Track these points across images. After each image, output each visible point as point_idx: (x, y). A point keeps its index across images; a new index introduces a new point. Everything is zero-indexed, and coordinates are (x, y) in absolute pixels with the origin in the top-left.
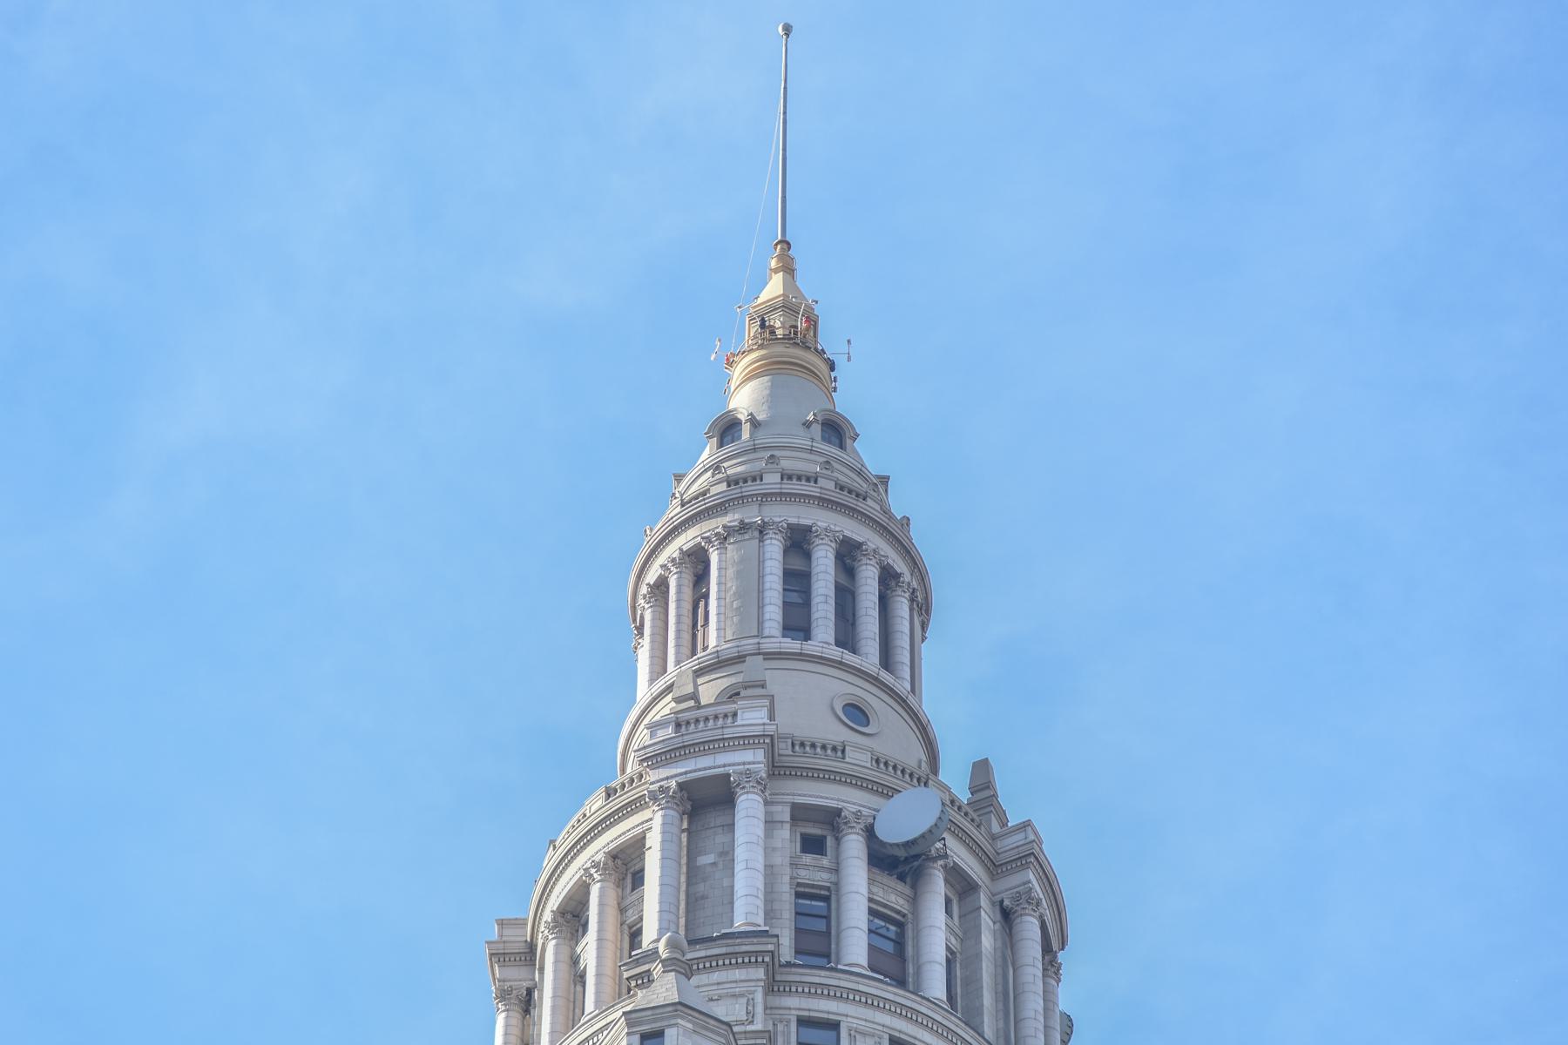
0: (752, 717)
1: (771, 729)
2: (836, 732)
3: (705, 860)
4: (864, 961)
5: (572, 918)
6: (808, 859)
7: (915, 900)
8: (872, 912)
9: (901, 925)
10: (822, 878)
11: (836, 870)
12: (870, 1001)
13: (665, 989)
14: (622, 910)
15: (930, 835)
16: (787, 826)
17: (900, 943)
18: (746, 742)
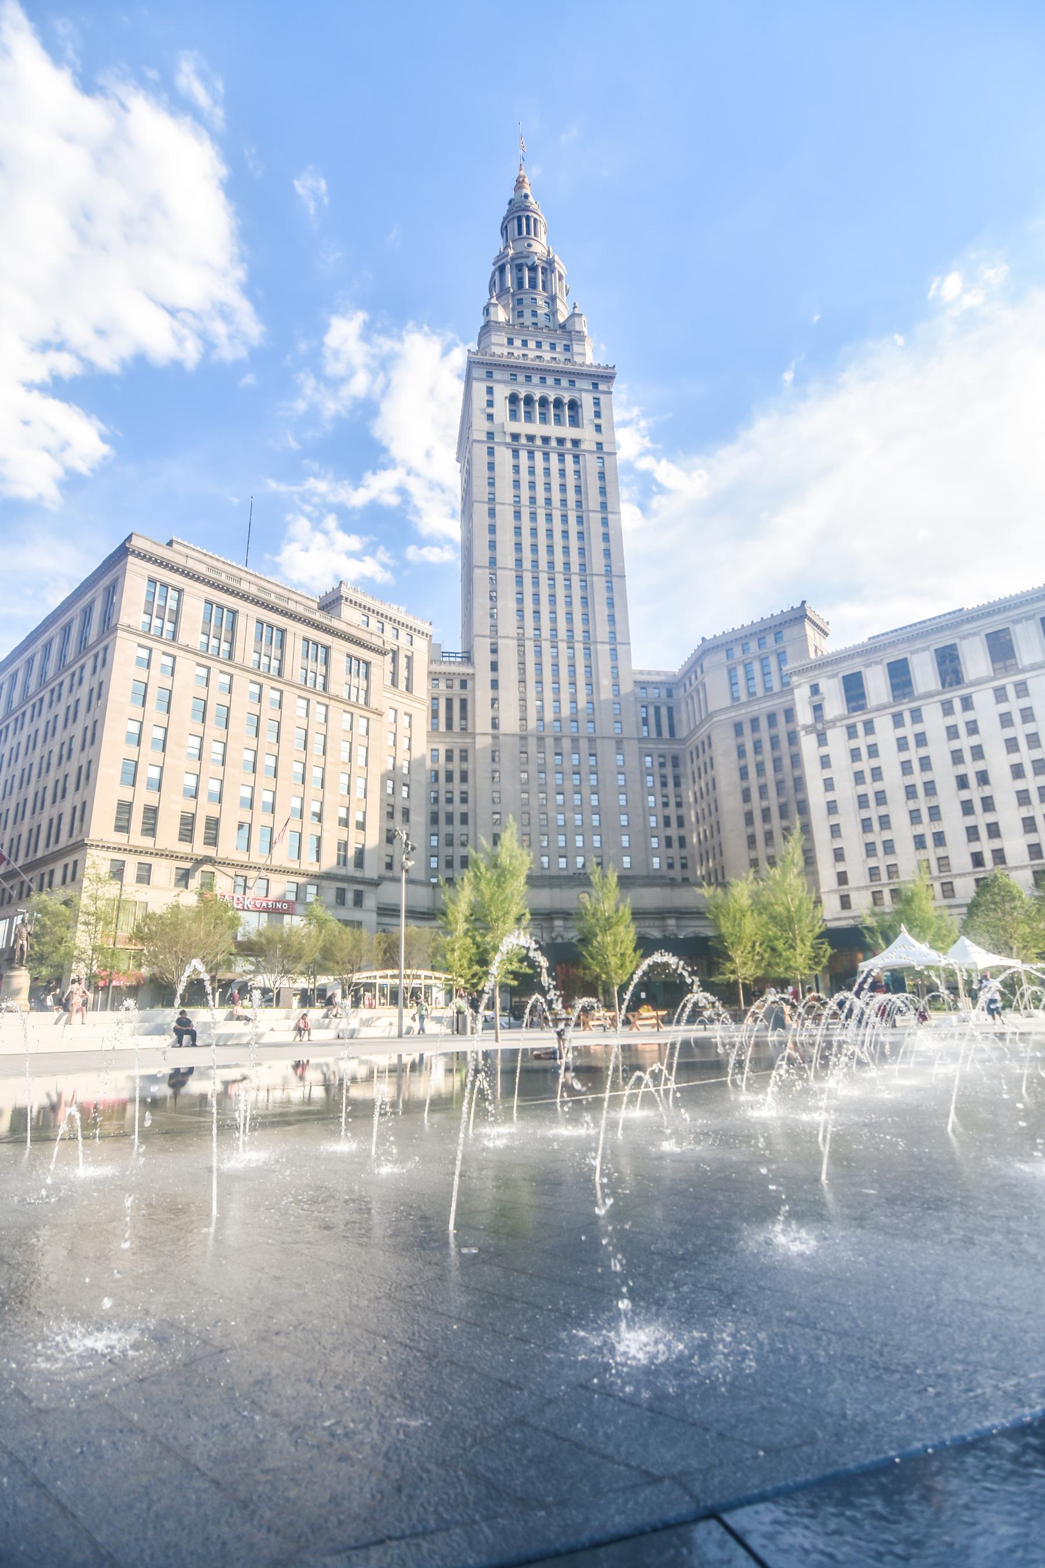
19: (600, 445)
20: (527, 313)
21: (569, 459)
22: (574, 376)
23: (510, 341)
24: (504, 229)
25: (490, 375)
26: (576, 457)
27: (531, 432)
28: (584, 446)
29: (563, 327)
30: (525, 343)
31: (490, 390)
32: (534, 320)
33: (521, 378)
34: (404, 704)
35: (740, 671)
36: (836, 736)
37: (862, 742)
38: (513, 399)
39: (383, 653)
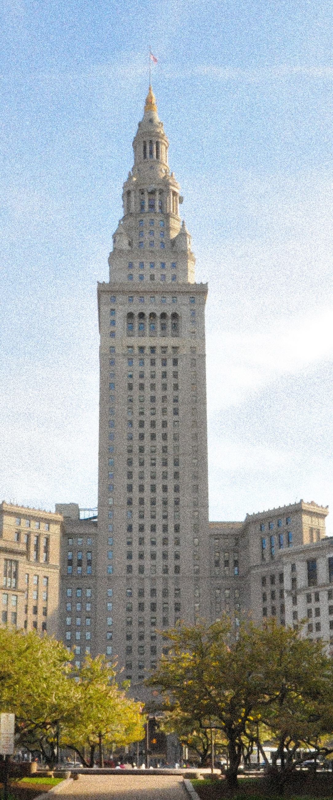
22: (174, 294)
23: (131, 265)
24: (135, 147)
25: (113, 299)
29: (173, 242)
30: (142, 265)
33: (136, 299)
34: (42, 572)
35: (267, 540)
36: (301, 599)
37: (313, 605)
38: (130, 315)
39: (27, 554)
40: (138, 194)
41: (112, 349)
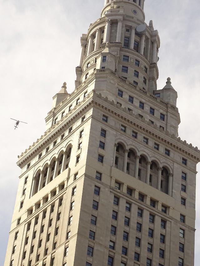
0: (121, 12)
1: (124, 14)
2: (133, 15)
3: (113, 31)
4: (133, 48)
5: (93, 36)
6: (127, 32)
7: (140, 40)
8: (135, 41)
9: (138, 43)
10: (128, 35)
11: (130, 34)
12: (133, 54)
13: (106, 50)
14: (100, 36)
15: (144, 31)
16: (125, 28)
17: (138, 45)
18: (120, 15)
19: (183, 218)
20: (131, 71)
21: (158, 220)
23: (121, 93)
25: (106, 119)
26: (164, 222)
27: (133, 186)
28: (171, 213)
30: (131, 99)
31: (104, 133)
32: (135, 79)
38: (120, 147)
40: (124, 29)
41: (99, 176)
